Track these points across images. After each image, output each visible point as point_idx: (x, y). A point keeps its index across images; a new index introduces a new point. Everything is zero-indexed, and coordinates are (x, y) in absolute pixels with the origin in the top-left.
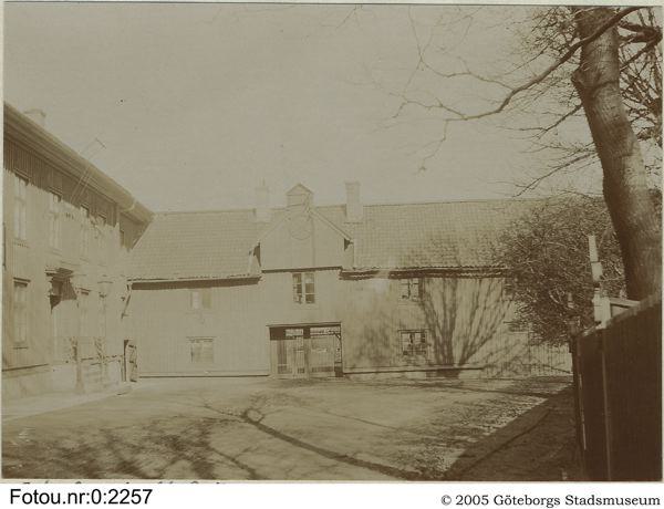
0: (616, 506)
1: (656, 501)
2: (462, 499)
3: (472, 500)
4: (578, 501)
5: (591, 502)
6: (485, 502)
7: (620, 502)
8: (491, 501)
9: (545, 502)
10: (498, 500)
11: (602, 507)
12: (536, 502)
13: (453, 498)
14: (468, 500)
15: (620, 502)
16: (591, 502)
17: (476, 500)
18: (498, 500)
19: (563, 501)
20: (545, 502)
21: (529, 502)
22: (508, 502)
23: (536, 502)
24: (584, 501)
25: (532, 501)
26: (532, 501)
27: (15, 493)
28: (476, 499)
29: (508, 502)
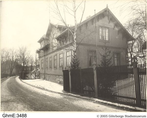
1: (145, 116)
2: (102, 116)
3: (104, 116)
4: (128, 116)
5: (130, 116)
6: (107, 116)
7: (137, 116)
10: (110, 116)
12: (118, 116)
13: (100, 115)
14: (103, 116)
15: (137, 116)
16: (130, 116)
17: (105, 116)
18: (110, 116)
19: (124, 116)
21: (117, 116)
22: (112, 116)
23: (118, 116)
24: (129, 117)
25: (117, 116)
26: (117, 116)
27: (14, 115)
29: (112, 116)
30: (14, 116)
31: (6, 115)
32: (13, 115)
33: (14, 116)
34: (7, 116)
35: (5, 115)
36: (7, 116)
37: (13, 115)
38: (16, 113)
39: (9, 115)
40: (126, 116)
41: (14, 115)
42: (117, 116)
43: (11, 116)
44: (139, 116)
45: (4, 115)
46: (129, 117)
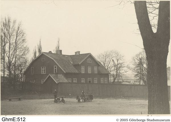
0: (159, 121)
1: (169, 120)
5: (153, 120)
6: (127, 120)
8: (128, 120)
9: (142, 120)
11: (156, 121)
16: (153, 120)
18: (130, 120)
19: (146, 120)
20: (142, 120)
21: (138, 120)
22: (133, 120)
24: (151, 120)
25: (139, 120)
26: (139, 120)
27: (14, 119)
28: (125, 120)
29: (133, 120)
30: (14, 120)
31: (5, 119)
32: (13, 119)
33: (14, 120)
34: (7, 119)
35: (4, 119)
36: (7, 119)
37: (13, 119)
38: (16, 117)
39: (9, 119)
40: (148, 120)
41: (14, 119)
42: (138, 120)
43: (11, 119)
44: (162, 120)
45: (4, 119)
46: (151, 120)
